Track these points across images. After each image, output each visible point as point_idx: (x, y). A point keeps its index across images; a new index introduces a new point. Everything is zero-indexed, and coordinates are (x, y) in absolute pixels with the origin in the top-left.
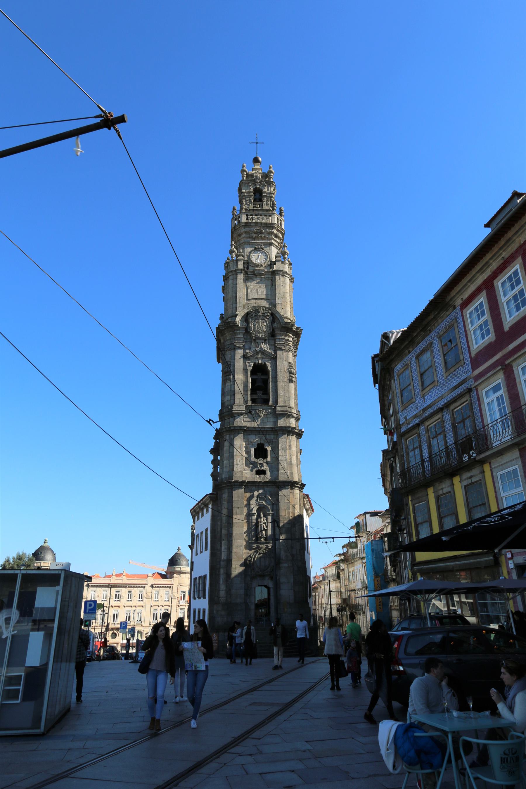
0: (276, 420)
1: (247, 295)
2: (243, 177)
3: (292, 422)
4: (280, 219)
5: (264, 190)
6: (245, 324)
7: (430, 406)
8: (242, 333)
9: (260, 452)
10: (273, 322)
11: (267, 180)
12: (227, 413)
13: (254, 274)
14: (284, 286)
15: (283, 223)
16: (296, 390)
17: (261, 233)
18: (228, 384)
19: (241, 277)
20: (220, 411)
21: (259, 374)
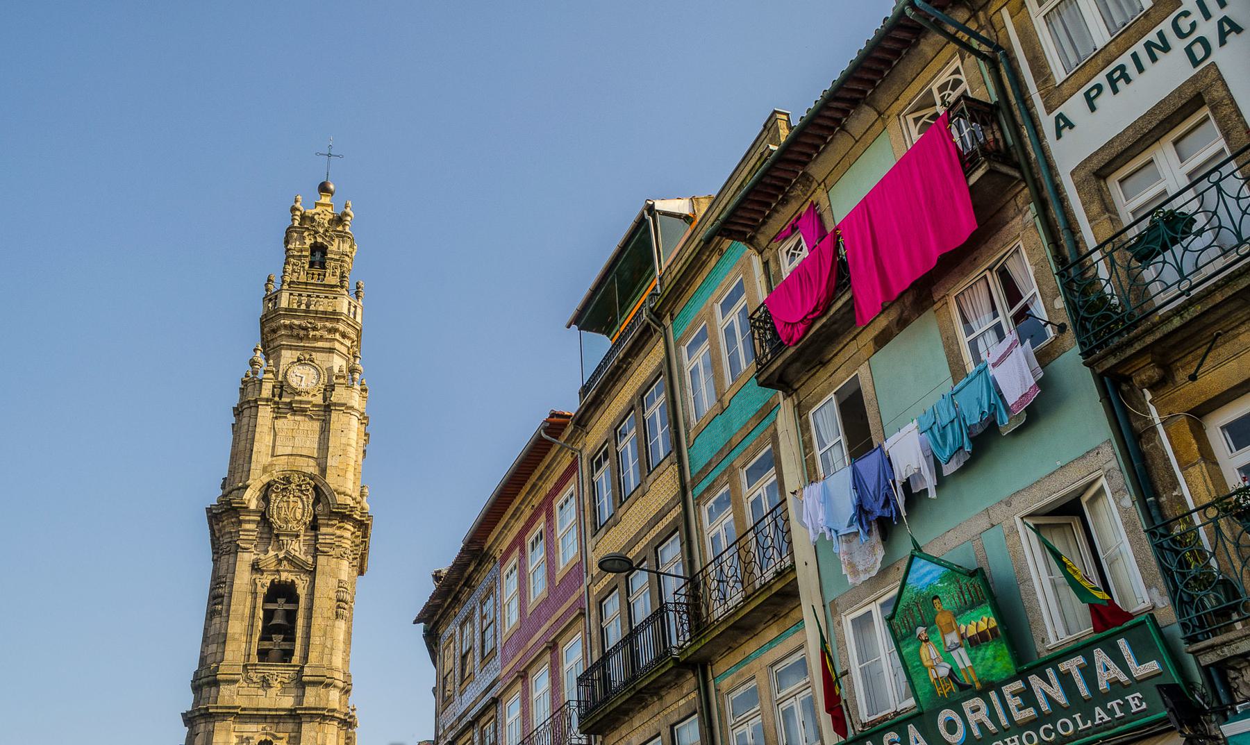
0: (300, 693)
1: (274, 447)
2: (293, 220)
3: (334, 698)
4: (353, 303)
5: (330, 248)
6: (263, 504)
7: (464, 714)
8: (254, 521)
10: (317, 501)
11: (340, 228)
12: (204, 680)
13: (292, 408)
14: (348, 433)
15: (359, 311)
16: (349, 633)
17: (315, 329)
18: (217, 620)
19: (265, 414)
20: (196, 673)
21: (281, 601)
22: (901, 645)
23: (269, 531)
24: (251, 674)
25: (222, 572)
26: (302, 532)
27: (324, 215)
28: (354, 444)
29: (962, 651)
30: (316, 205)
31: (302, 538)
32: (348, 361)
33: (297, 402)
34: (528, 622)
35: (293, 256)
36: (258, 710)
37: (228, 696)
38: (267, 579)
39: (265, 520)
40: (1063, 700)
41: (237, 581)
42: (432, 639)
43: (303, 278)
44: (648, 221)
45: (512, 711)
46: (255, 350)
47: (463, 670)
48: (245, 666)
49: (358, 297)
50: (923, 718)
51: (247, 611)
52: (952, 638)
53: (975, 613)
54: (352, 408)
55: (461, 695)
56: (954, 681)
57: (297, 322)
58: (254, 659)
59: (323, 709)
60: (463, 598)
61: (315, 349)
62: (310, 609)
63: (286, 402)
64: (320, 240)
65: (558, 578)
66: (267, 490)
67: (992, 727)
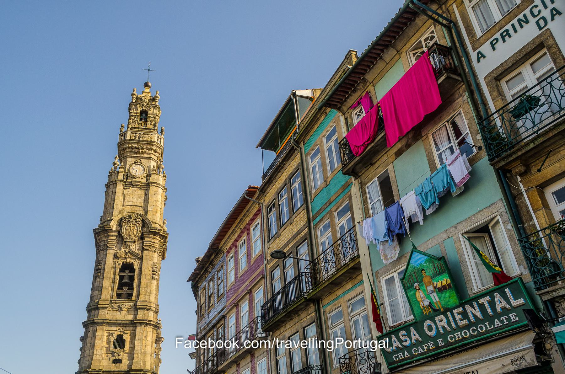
1: (124, 202)
2: (132, 99)
3: (151, 315)
4: (160, 137)
5: (149, 112)
6: (119, 228)
9: (120, 342)
10: (143, 226)
11: (154, 103)
12: (92, 307)
13: (132, 184)
14: (158, 195)
15: (162, 140)
16: (158, 286)
17: (142, 148)
18: (98, 280)
19: (120, 187)
20: (89, 304)
22: (407, 291)
23: (122, 240)
24: (114, 304)
25: (100, 259)
26: (137, 240)
27: (146, 97)
28: (160, 201)
29: (435, 294)
30: (143, 92)
31: (136, 243)
32: (157, 163)
33: (134, 181)
34: (239, 281)
35: (133, 116)
36: (117, 320)
37: (103, 314)
38: (121, 262)
39: (120, 235)
40: (480, 316)
41: (107, 263)
42: (195, 289)
43: (137, 126)
44: (293, 100)
45: (231, 321)
46: (115, 158)
47: (209, 303)
48: (111, 301)
49: (162, 134)
50: (417, 325)
51: (112, 276)
52: (430, 288)
53: (441, 277)
54: (159, 184)
55: (208, 314)
56: (431, 308)
57: (134, 145)
58: (115, 298)
59: (146, 320)
60: (209, 270)
61: (143, 158)
62: (140, 275)
63: (129, 181)
64: (144, 108)
65: (252, 261)
66: (121, 221)
67: (448, 329)
